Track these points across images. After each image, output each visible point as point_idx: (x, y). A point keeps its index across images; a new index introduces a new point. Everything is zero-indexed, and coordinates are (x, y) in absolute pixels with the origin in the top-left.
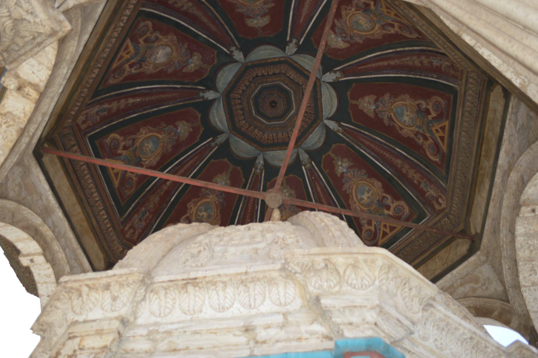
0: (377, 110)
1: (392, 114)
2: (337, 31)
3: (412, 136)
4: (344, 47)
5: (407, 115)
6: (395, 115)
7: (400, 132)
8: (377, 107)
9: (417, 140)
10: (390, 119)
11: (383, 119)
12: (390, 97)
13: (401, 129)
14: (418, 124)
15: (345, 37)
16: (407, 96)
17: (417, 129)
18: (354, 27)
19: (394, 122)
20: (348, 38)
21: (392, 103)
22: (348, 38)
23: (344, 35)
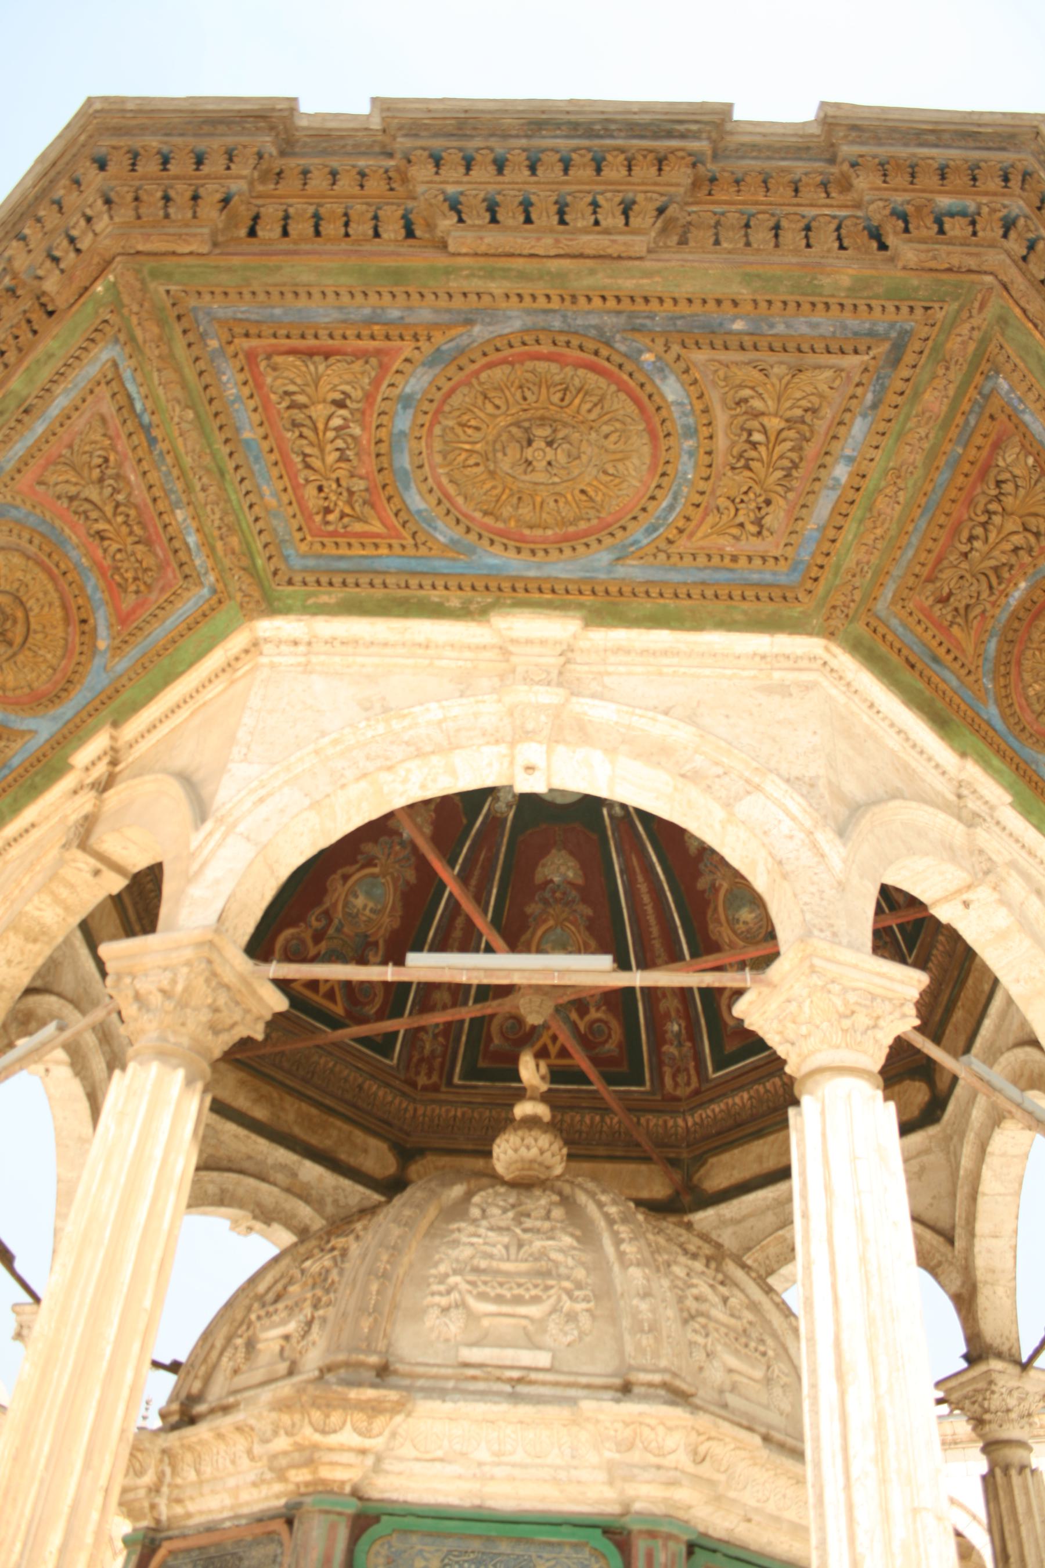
0: (396, 839)
1: (376, 870)
2: (574, 893)
3: (327, 903)
4: (539, 869)
5: (365, 907)
6: (374, 876)
7: (340, 872)
8: (402, 844)
9: (318, 911)
10: (370, 863)
11: (376, 842)
12: (407, 883)
13: (346, 878)
14: (346, 930)
15: (554, 892)
16: (396, 924)
17: (336, 922)
18: (559, 930)
19: (363, 867)
20: (547, 894)
21: (395, 880)
22: (547, 894)
23: (558, 895)
